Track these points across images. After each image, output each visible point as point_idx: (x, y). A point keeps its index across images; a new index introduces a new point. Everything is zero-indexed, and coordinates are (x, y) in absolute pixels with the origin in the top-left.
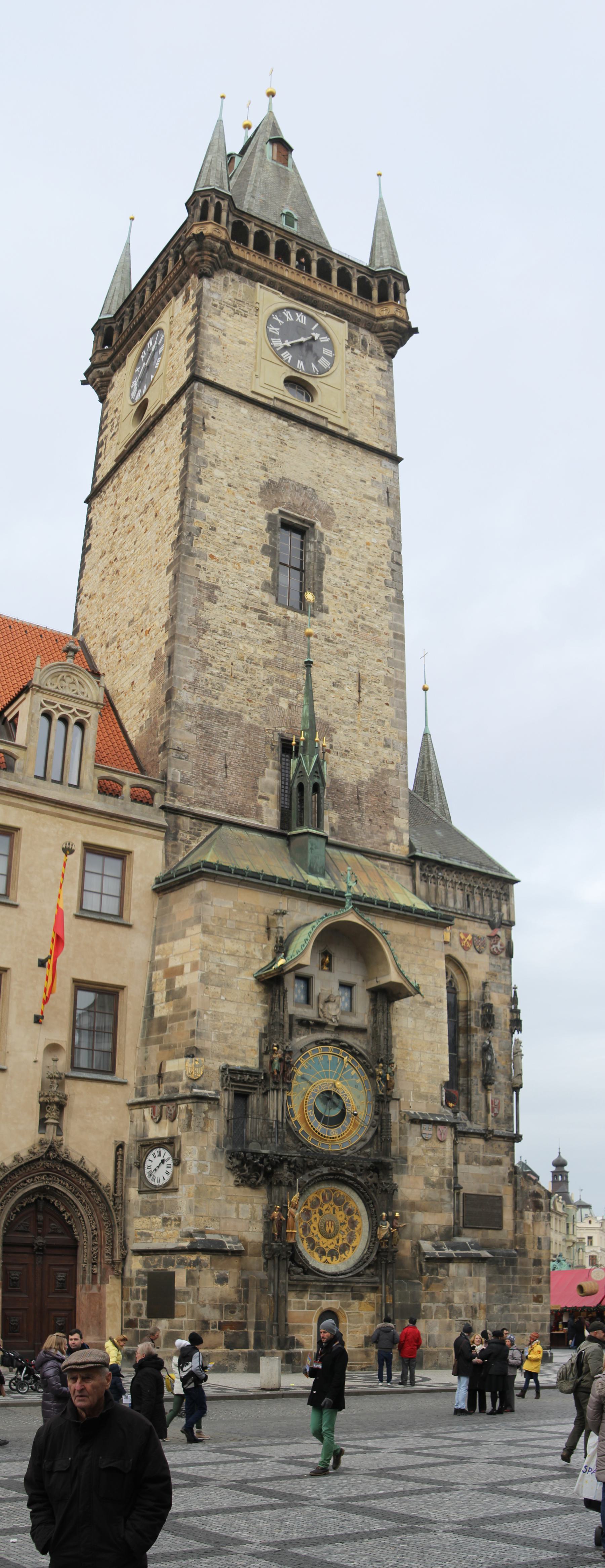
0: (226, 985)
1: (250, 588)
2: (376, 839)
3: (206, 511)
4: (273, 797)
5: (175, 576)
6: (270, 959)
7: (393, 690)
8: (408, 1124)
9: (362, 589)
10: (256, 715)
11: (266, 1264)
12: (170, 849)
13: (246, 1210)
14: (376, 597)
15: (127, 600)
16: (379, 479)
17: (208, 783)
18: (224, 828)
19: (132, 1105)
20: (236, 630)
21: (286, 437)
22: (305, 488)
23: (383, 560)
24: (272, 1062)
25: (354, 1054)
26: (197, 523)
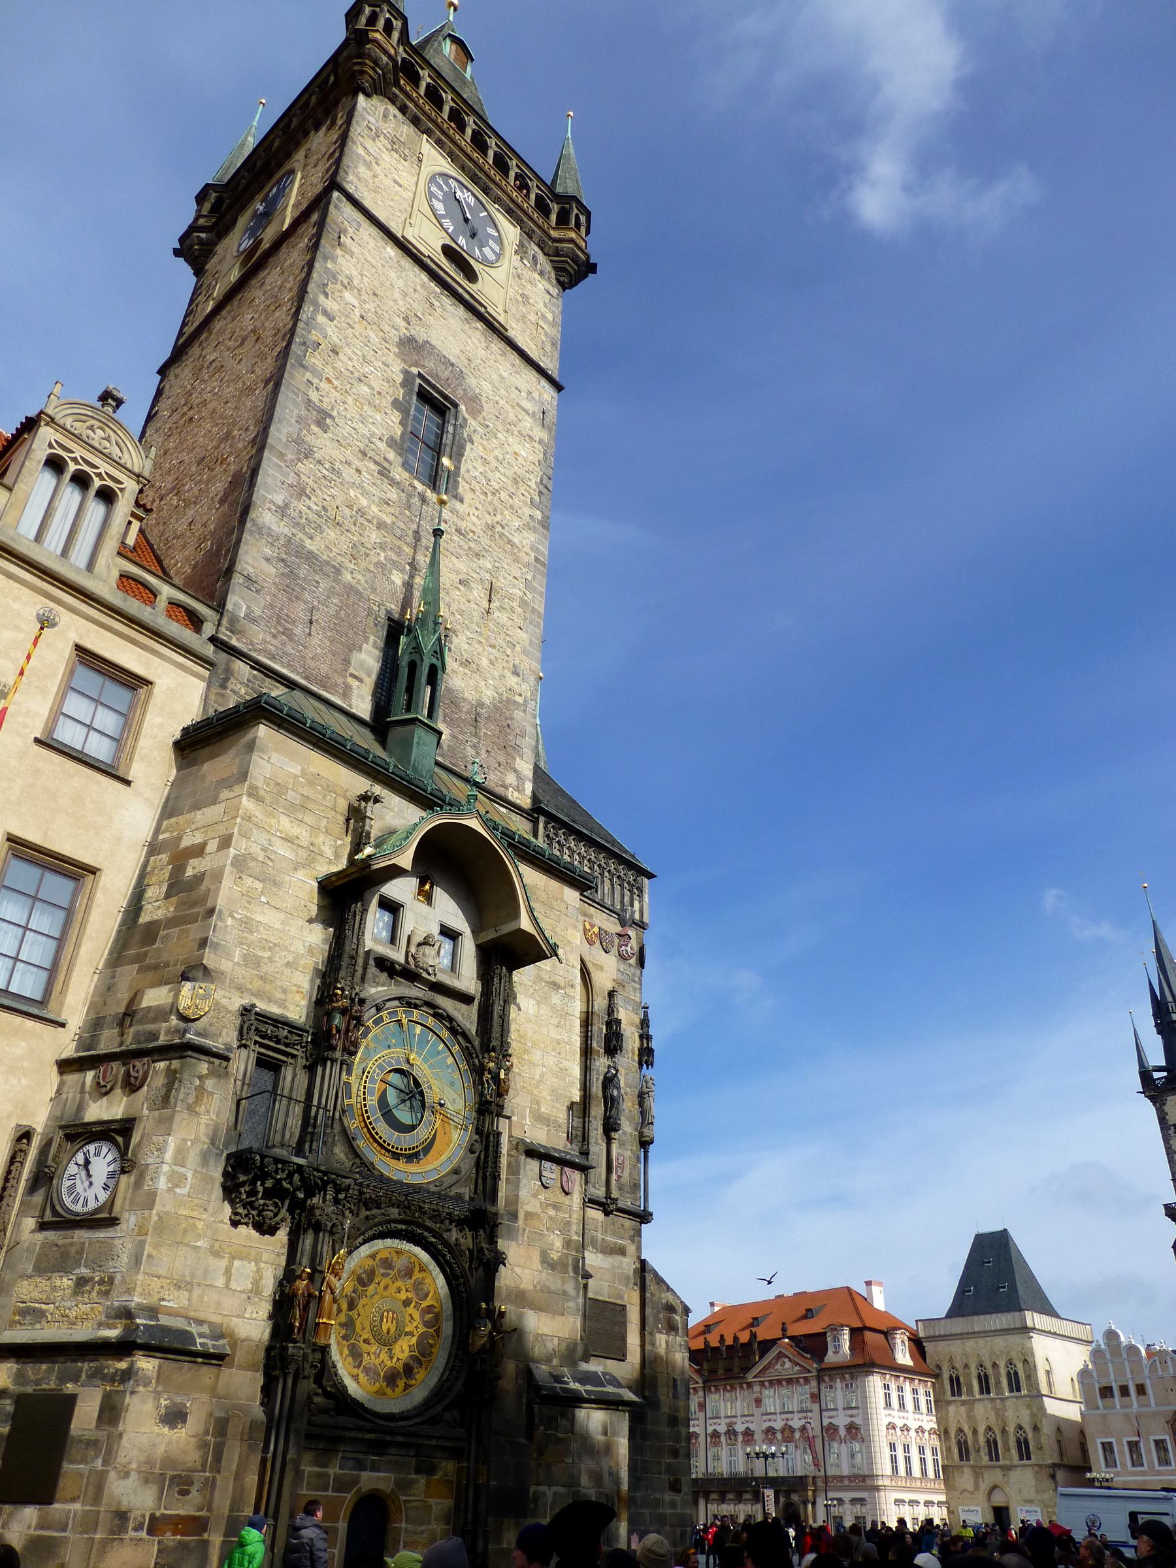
0: (271, 882)
3: (329, 329)
4: (370, 681)
7: (528, 615)
9: (504, 495)
10: (360, 577)
12: (212, 697)
13: (244, 1272)
16: (536, 395)
17: (283, 633)
19: (65, 1066)
20: (348, 474)
21: (436, 303)
22: (452, 365)
23: (531, 477)
26: (314, 336)
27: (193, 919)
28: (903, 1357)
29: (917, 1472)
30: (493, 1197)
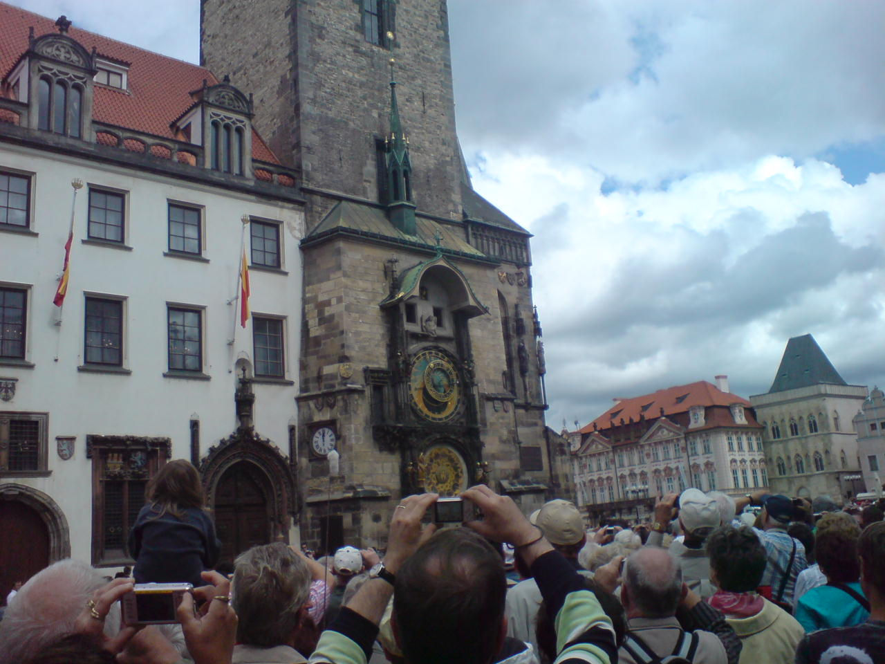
0: (362, 312)
2: (441, 210)
4: (374, 180)
5: (294, 20)
6: (388, 293)
8: (485, 401)
9: (421, 31)
18: (344, 203)
19: (298, 400)
23: (434, 9)
24: (397, 364)
27: (335, 336)
28: (740, 419)
29: (751, 484)
30: (475, 421)
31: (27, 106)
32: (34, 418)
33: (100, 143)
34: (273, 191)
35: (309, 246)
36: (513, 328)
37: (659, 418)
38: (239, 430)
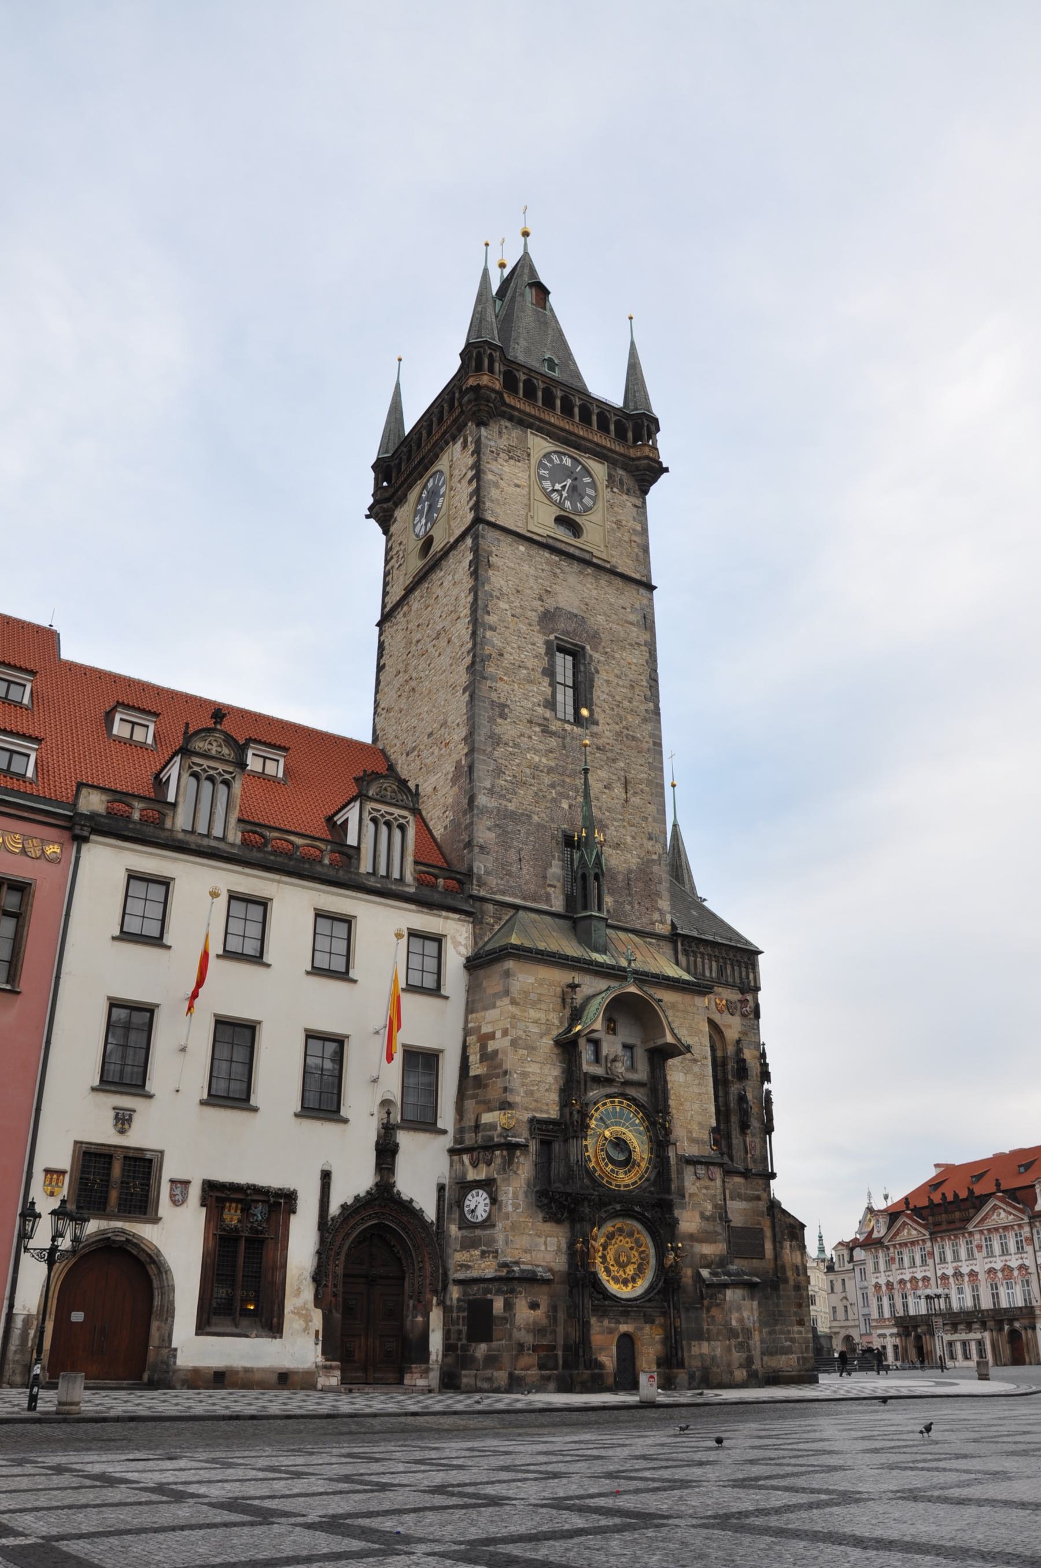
0: (532, 1048)
1: (534, 705)
4: (558, 885)
5: (471, 696)
6: (566, 1025)
9: (626, 704)
11: (571, 1291)
12: (477, 931)
13: (553, 1241)
14: (638, 710)
15: (425, 715)
16: (637, 606)
18: (520, 912)
19: (452, 1152)
22: (576, 616)
24: (571, 1114)
25: (637, 1105)
30: (668, 1191)
31: (174, 805)
32: (148, 1156)
33: (244, 842)
34: (436, 898)
35: (477, 964)
36: (732, 1071)
37: (994, 1193)
38: (377, 1185)
